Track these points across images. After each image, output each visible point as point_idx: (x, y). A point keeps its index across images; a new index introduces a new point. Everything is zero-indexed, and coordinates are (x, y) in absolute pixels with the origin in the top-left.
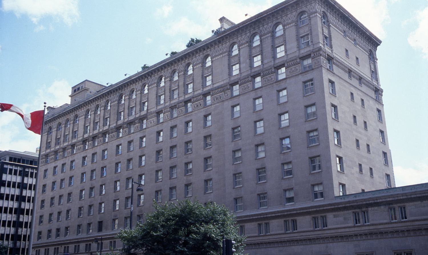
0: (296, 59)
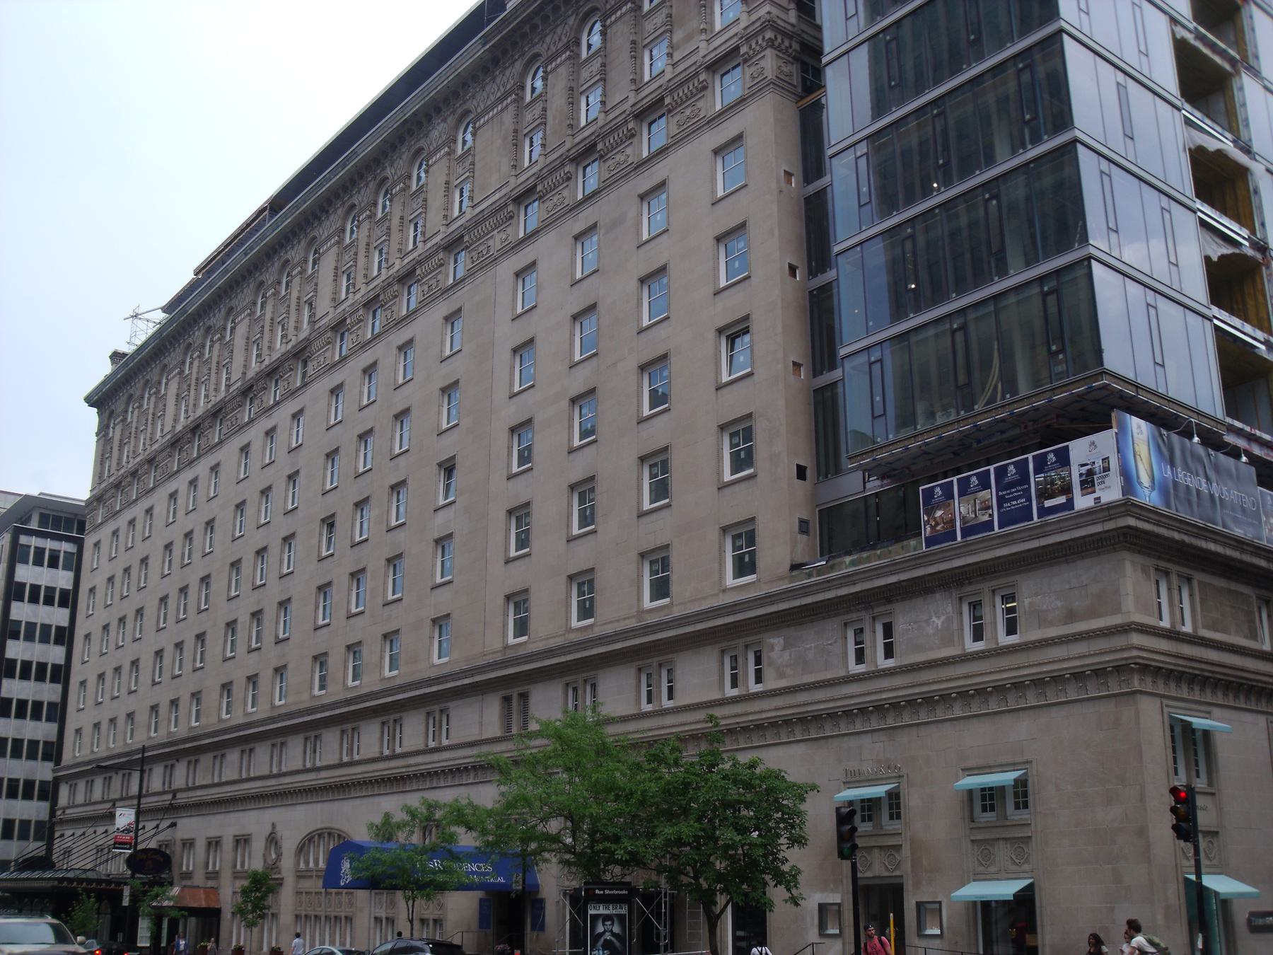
0: (697, 74)
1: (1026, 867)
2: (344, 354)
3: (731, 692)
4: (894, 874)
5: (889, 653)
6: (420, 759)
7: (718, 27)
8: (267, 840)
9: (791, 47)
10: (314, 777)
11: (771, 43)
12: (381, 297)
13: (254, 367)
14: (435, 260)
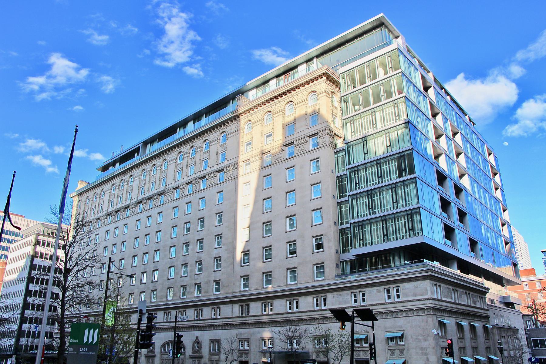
3: (316, 308)
11: (328, 134)
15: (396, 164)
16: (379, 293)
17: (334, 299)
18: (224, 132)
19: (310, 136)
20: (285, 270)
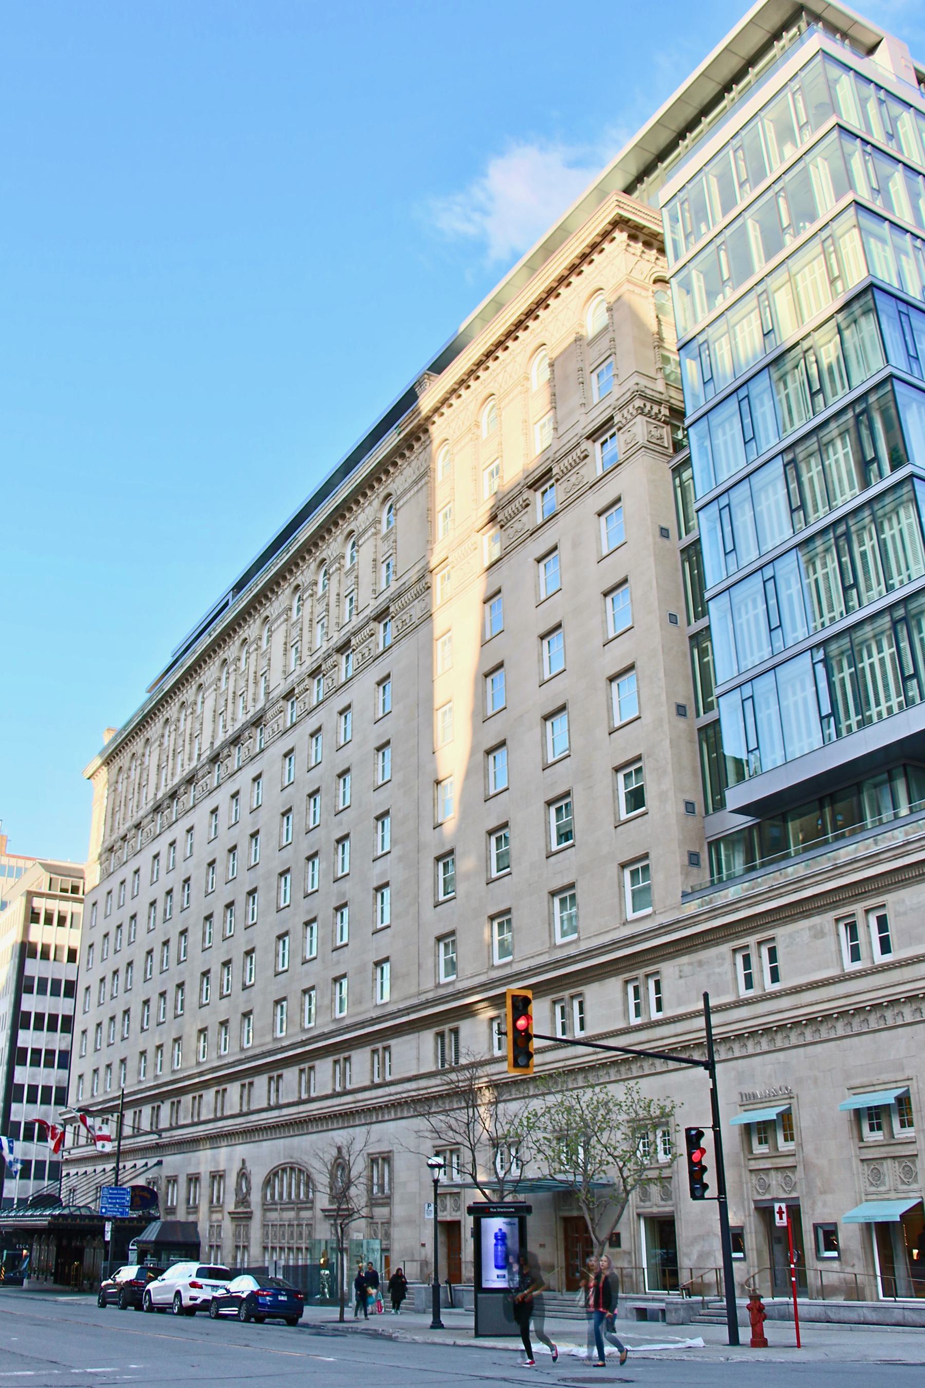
1: (914, 1186)
2: (294, 721)
4: (763, 1198)
5: (775, 978)
6: (367, 1095)
7: (596, 401)
8: (238, 1174)
9: (660, 412)
10: (277, 1115)
11: (641, 411)
12: (323, 667)
13: (221, 738)
14: (366, 631)
15: (849, 449)
16: (819, 942)
17: (682, 981)
18: (389, 495)
19: (592, 436)
20: (545, 895)
